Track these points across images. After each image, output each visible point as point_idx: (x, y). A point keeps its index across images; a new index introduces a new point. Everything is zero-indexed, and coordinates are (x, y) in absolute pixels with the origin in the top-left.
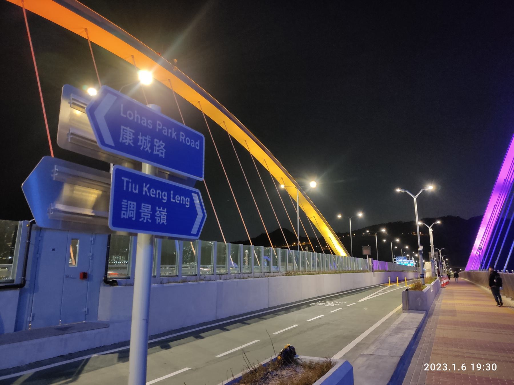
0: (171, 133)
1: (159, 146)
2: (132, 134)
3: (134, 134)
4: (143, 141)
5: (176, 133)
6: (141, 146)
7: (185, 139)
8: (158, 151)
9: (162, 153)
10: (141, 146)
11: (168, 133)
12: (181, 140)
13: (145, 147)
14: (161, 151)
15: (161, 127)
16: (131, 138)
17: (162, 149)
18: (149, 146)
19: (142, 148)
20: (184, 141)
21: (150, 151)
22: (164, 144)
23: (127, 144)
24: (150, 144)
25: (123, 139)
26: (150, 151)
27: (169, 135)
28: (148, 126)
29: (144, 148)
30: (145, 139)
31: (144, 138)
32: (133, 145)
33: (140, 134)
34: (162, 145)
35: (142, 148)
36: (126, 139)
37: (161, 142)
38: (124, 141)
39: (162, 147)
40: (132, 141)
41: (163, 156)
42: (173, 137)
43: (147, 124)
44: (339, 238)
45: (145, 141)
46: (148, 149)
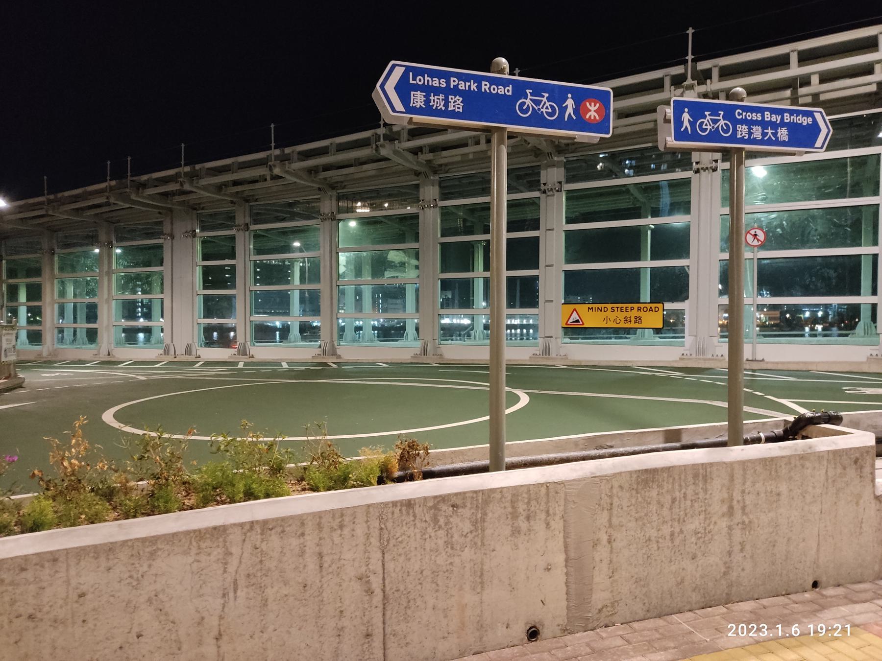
0: (470, 86)
1: (455, 102)
2: (423, 96)
3: (424, 96)
4: (436, 100)
5: (476, 84)
6: (434, 105)
7: (489, 89)
8: (454, 106)
9: (459, 108)
10: (434, 105)
11: (465, 87)
12: (483, 91)
13: (438, 105)
14: (457, 106)
15: (456, 83)
16: (423, 101)
17: (458, 104)
18: (442, 103)
19: (434, 108)
20: (488, 91)
21: (443, 108)
22: (461, 99)
23: (418, 107)
24: (444, 101)
25: (414, 103)
26: (443, 108)
27: (467, 89)
28: (441, 85)
29: (437, 107)
30: (438, 99)
31: (436, 97)
32: (424, 107)
33: (432, 94)
34: (459, 100)
35: (434, 108)
36: (417, 102)
37: (457, 97)
38: (414, 105)
39: (459, 102)
40: (423, 103)
41: (461, 110)
42: (472, 89)
43: (440, 83)
44: (628, 176)
45: (438, 101)
46: (441, 106)
